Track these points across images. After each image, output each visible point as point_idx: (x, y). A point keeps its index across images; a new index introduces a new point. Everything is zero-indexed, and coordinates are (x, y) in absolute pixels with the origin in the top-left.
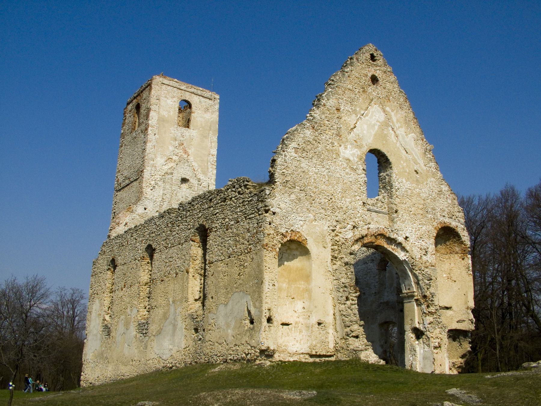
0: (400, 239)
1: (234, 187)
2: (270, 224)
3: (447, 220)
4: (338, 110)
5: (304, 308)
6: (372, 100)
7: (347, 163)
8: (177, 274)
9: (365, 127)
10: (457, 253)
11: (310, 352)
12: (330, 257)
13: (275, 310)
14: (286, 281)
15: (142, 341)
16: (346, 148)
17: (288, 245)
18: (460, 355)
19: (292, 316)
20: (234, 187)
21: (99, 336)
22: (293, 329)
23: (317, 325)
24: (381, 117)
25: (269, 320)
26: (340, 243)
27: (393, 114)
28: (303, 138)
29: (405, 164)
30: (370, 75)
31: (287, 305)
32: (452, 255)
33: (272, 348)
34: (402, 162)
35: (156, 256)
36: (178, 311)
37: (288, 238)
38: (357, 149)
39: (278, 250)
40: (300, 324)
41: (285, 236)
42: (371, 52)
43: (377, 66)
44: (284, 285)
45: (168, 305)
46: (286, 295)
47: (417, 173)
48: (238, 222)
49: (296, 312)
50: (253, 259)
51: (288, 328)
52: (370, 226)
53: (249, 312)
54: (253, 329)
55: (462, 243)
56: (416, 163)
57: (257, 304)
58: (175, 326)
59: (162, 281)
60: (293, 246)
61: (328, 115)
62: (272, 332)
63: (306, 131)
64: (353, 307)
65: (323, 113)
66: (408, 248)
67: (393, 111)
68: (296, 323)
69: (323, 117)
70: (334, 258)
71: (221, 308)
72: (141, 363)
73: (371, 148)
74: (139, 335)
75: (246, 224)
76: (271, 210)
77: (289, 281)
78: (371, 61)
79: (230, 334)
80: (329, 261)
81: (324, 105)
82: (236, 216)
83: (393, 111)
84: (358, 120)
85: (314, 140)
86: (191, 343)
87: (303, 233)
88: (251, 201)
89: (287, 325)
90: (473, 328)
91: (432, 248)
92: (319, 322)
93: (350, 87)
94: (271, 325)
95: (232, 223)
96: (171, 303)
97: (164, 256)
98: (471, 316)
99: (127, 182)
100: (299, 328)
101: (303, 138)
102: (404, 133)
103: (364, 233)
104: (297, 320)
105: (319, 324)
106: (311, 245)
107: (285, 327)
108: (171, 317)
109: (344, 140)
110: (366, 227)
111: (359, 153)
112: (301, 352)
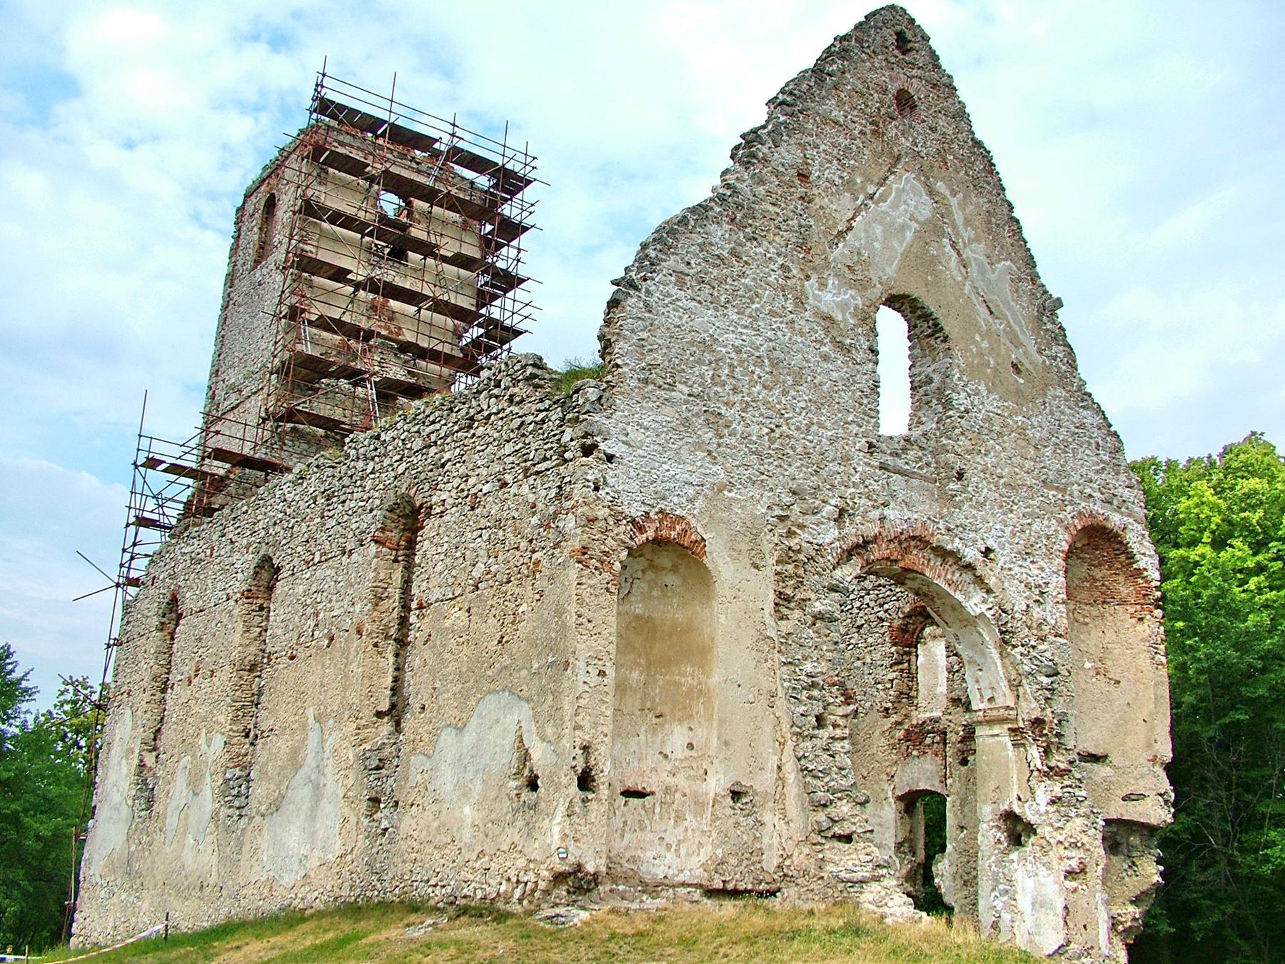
0: (971, 554)
1: (498, 385)
2: (597, 489)
3: (1098, 508)
4: (803, 176)
5: (690, 746)
6: (898, 159)
7: (826, 330)
8: (332, 639)
9: (879, 230)
10: (1123, 602)
11: (704, 882)
12: (772, 597)
13: (603, 749)
14: (639, 664)
15: (228, 829)
16: (823, 285)
17: (648, 556)
18: (1132, 895)
19: (654, 769)
20: (498, 385)
21: (125, 811)
22: (658, 810)
23: (729, 801)
24: (925, 209)
25: (585, 781)
26: (801, 557)
27: (954, 202)
28: (702, 247)
29: (985, 345)
30: (893, 88)
31: (642, 737)
32: (1109, 609)
33: (590, 868)
34: (978, 338)
35: (281, 588)
36: (328, 747)
37: (651, 534)
38: (853, 292)
39: (617, 566)
40: (678, 795)
41: (641, 529)
42: (898, 28)
43: (912, 65)
44: (635, 675)
45: (304, 726)
46: (638, 704)
47: (1018, 371)
48: (505, 485)
49: (666, 756)
50: (541, 593)
51: (644, 807)
52: (886, 512)
53: (526, 757)
54: (534, 807)
55: (1139, 573)
56: (1017, 344)
57: (550, 731)
58: (317, 788)
59: (292, 658)
60: (665, 560)
61: (773, 187)
62: (592, 817)
63: (713, 228)
64: (837, 746)
65: (762, 182)
66: (992, 581)
67: (954, 194)
68: (667, 790)
69: (761, 190)
70: (783, 600)
71: (448, 737)
72: (224, 892)
73: (894, 292)
74: (225, 811)
75: (525, 489)
76: (602, 446)
77: (649, 663)
78: (896, 52)
79: (469, 821)
80: (769, 607)
81: (765, 160)
82: (497, 468)
83: (954, 194)
84: (857, 211)
85: (733, 253)
86: (362, 843)
87: (693, 522)
88: (543, 421)
89: (641, 795)
90: (1169, 819)
91: (1057, 584)
92: (737, 789)
93: (837, 114)
94: (591, 796)
95: (486, 488)
96: (311, 720)
97: (301, 589)
98: (1166, 785)
99: (234, 399)
100: (675, 807)
101: (702, 247)
102: (982, 258)
103: (871, 530)
104: (671, 781)
105: (736, 795)
106: (718, 558)
107: (634, 802)
108: (310, 761)
109: (817, 261)
110: (875, 514)
111: (859, 302)
112: (681, 878)
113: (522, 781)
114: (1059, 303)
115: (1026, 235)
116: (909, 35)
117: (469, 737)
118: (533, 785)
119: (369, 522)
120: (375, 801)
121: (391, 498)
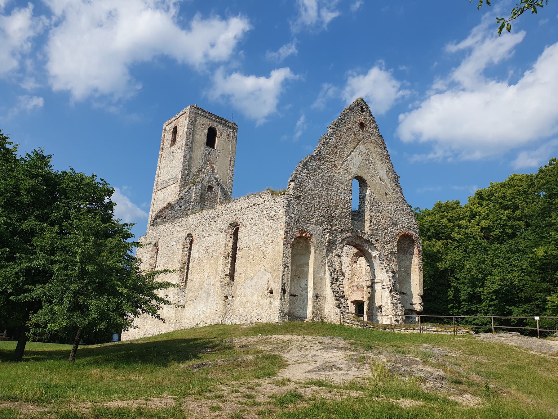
0: (373, 241)
6: (360, 141)
23: (315, 298)
57: (276, 280)
89: (295, 296)
99: (165, 185)
113: (268, 291)
114: (399, 177)
115: (391, 159)
116: (364, 107)
117: (254, 281)
118: (271, 292)
119: (225, 226)
120: (227, 297)
121: (230, 221)
